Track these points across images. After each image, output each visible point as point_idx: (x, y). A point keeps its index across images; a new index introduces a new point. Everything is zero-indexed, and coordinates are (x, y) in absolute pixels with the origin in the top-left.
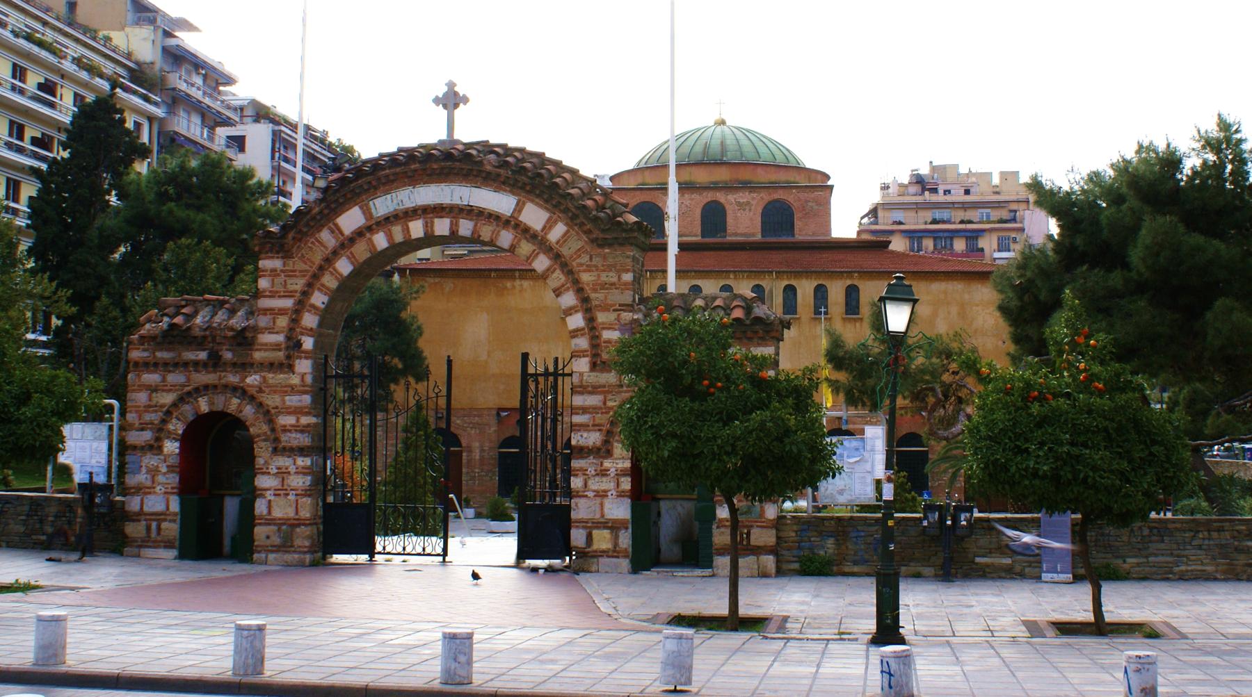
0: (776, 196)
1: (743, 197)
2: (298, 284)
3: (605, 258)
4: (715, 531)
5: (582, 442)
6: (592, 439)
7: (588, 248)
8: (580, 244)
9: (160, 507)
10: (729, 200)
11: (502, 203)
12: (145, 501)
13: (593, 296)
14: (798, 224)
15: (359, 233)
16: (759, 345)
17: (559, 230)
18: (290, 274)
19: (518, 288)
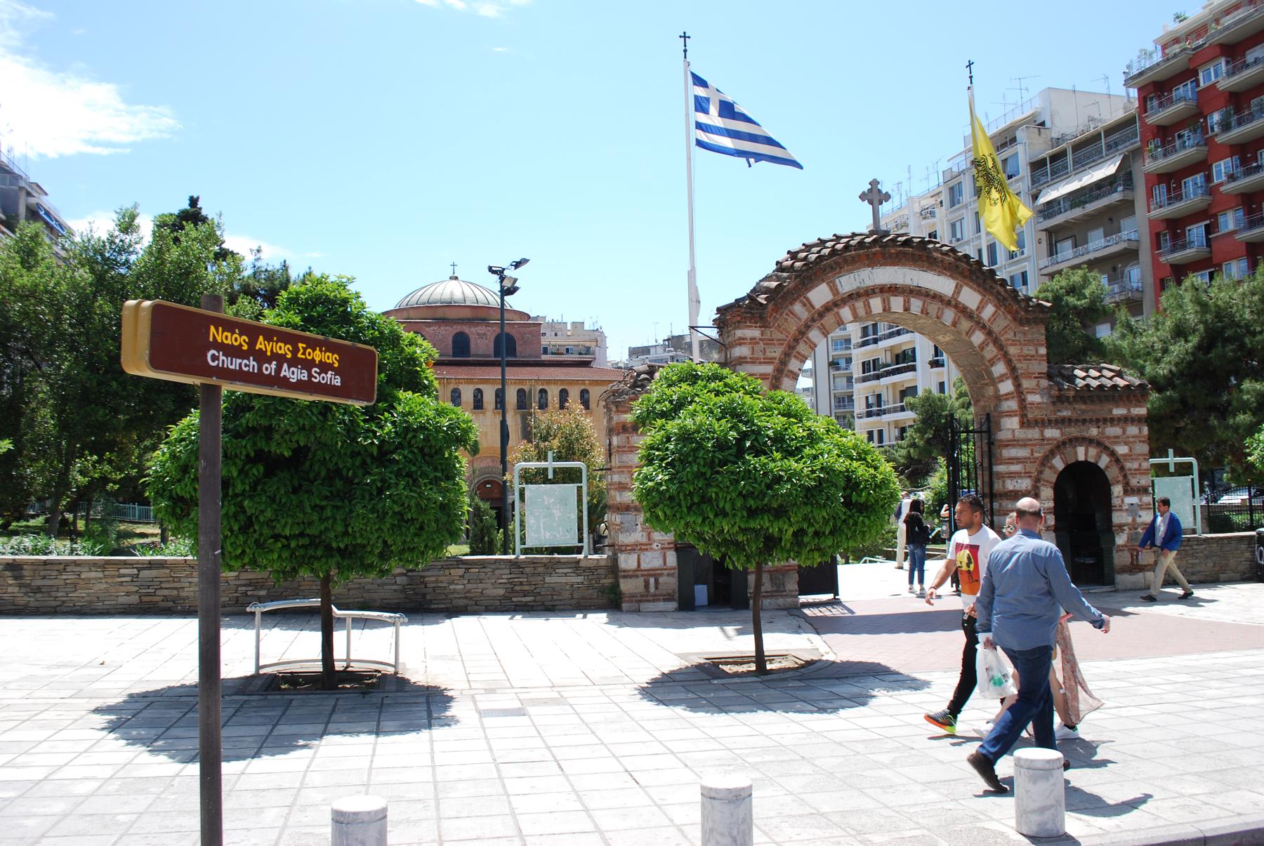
1: (481, 329)
2: (776, 352)
3: (1025, 333)
4: (1115, 555)
5: (1018, 487)
6: (1025, 484)
7: (1013, 325)
8: (1007, 322)
9: (657, 563)
10: (471, 331)
11: (943, 284)
12: (642, 557)
13: (1018, 365)
14: (519, 349)
15: (827, 308)
16: (1136, 406)
17: (989, 311)
18: (769, 342)
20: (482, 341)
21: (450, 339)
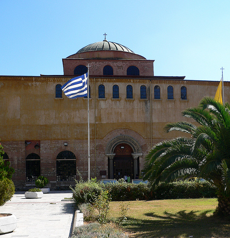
0: (132, 64)
1: (120, 64)
19: (34, 85)
20: (120, 69)
21: (102, 69)
